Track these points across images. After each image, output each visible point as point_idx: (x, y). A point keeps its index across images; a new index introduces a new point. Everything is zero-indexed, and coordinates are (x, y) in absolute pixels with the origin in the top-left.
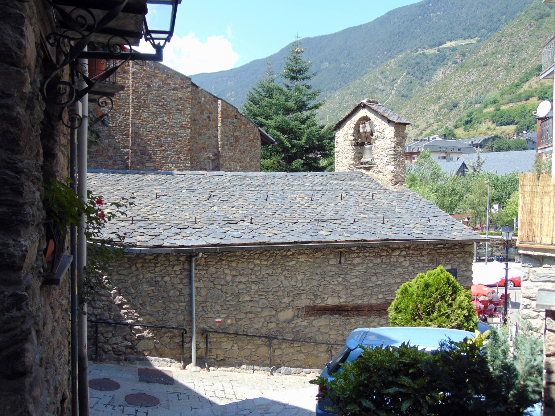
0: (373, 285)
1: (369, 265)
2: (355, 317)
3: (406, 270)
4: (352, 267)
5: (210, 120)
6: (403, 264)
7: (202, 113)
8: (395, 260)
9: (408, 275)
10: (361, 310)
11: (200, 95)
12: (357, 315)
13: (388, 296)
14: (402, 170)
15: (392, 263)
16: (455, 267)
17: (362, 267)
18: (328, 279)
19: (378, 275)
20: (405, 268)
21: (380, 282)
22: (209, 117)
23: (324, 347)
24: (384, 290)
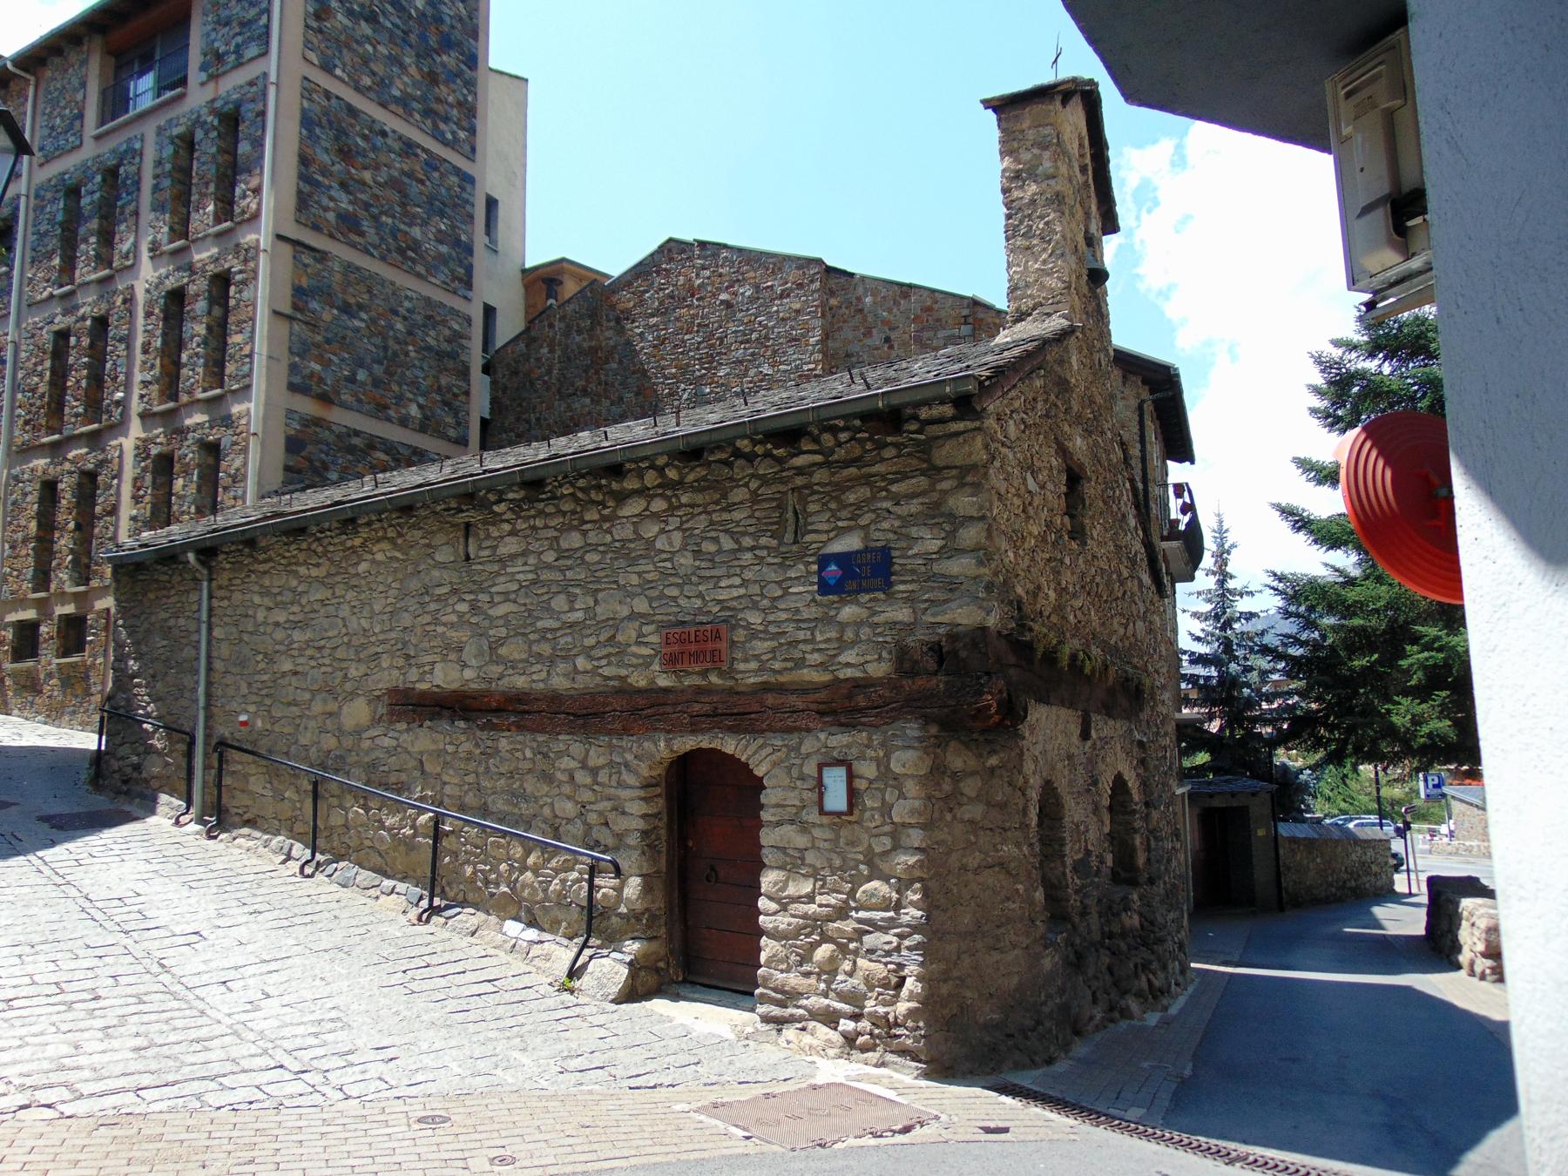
2: (513, 733)
3: (668, 565)
4: (496, 567)
5: (891, 347)
7: (868, 334)
8: (627, 532)
9: (677, 585)
10: (528, 712)
11: (860, 290)
12: (520, 728)
13: (604, 662)
14: (1044, 262)
15: (617, 544)
16: (880, 537)
17: (525, 564)
18: (433, 606)
19: (571, 589)
21: (579, 615)
22: (887, 340)
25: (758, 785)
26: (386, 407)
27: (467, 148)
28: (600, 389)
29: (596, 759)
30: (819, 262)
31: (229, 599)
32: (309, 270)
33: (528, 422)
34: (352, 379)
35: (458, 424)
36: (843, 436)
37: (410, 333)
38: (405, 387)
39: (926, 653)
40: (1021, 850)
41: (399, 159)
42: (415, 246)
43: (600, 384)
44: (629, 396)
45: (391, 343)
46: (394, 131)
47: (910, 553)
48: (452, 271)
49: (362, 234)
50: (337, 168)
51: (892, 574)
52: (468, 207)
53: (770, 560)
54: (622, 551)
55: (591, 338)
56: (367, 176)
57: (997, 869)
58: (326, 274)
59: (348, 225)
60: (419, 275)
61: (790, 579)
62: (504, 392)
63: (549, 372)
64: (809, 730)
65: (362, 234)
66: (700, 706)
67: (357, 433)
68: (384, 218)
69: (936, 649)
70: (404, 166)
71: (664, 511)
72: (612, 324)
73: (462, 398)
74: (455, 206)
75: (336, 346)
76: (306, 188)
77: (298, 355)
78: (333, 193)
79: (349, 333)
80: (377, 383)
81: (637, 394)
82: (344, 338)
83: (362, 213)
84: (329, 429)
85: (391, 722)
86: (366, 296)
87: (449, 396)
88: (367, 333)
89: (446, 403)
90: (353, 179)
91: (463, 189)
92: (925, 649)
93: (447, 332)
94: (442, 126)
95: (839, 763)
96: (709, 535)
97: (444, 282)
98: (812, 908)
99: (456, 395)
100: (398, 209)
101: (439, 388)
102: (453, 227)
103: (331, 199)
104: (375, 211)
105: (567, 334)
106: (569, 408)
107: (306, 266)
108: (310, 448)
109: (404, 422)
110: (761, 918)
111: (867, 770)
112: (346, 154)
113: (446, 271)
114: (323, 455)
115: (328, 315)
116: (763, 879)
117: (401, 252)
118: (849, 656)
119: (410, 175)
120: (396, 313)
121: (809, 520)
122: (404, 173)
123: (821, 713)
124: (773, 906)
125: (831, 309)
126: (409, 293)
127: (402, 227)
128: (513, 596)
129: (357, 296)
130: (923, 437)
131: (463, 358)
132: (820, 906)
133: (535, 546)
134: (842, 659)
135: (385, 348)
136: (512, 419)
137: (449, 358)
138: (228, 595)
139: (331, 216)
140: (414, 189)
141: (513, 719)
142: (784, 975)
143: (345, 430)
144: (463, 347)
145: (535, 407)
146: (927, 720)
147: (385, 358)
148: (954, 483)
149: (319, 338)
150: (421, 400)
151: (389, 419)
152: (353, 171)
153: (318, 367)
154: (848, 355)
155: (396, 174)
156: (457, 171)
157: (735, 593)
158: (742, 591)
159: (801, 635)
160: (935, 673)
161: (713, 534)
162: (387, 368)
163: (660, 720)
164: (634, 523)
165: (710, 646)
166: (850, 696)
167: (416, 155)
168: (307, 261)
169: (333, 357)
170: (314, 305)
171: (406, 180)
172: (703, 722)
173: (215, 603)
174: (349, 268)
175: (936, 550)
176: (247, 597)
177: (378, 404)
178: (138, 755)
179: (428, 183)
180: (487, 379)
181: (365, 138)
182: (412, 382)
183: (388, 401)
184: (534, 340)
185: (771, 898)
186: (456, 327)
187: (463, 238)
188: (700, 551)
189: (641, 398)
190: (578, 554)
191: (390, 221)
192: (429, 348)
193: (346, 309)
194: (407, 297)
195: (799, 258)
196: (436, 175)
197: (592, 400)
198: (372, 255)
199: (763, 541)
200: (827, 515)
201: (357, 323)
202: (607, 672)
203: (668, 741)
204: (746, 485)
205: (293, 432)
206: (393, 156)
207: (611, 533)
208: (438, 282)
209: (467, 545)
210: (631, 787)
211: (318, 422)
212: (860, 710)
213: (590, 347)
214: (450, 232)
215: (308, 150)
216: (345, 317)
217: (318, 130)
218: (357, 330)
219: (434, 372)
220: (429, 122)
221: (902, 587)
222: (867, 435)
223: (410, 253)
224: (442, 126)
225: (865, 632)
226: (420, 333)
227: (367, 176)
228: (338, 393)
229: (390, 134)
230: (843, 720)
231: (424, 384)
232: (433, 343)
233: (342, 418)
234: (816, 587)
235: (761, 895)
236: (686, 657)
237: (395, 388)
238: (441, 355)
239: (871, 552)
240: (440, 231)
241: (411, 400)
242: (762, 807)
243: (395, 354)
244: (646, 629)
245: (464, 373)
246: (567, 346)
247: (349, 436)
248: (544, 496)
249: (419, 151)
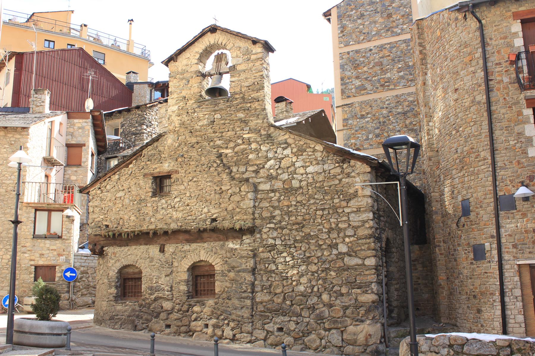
42: (389, 80)
49: (366, 89)
56: (365, 69)
93: (407, 103)
97: (403, 86)
101: (406, 125)
102: (405, 63)
117: (382, 86)
122: (381, 58)
126: (387, 98)
149: (353, 131)
152: (360, 71)
171: (381, 60)
192: (399, 113)
198: (371, 94)
224: (395, 30)
227: (365, 69)
243: (384, 122)
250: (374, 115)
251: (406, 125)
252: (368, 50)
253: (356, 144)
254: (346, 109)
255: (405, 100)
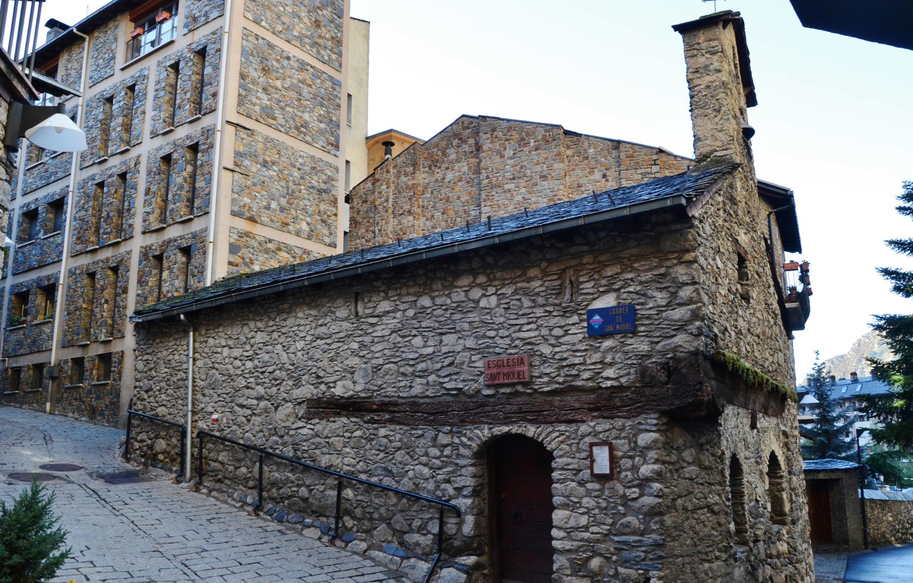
0: (416, 355)
1: (407, 314)
3: (488, 317)
5: (607, 180)
6: (483, 303)
8: (462, 296)
9: (495, 330)
11: (586, 145)
12: (391, 421)
13: (447, 379)
15: (455, 305)
17: (394, 318)
19: (424, 333)
20: (488, 313)
21: (430, 350)
23: (331, 481)
24: (439, 366)
25: (550, 456)
26: (287, 224)
27: (337, 64)
28: (419, 210)
29: (444, 439)
30: (559, 127)
31: (206, 342)
32: (244, 141)
33: (374, 232)
34: (268, 208)
35: (331, 234)
36: (602, 234)
37: (302, 178)
38: (299, 212)
39: (659, 371)
40: (721, 498)
41: (297, 73)
42: (305, 125)
43: (419, 207)
44: (438, 214)
45: (291, 184)
46: (294, 57)
47: (648, 307)
48: (327, 139)
49: (274, 119)
50: (261, 80)
51: (636, 320)
52: (337, 100)
53: (555, 314)
54: (459, 307)
55: (413, 179)
56: (278, 84)
57: (706, 510)
58: (253, 143)
59: (267, 114)
60: (307, 143)
61: (569, 324)
62: (358, 214)
63: (387, 201)
64: (583, 422)
65: (274, 119)
66: (510, 407)
67: (270, 241)
68: (288, 109)
69: (665, 366)
70: (300, 76)
71: (484, 283)
72: (427, 169)
73: (333, 218)
74: (330, 99)
75: (259, 187)
76: (243, 93)
77: (237, 193)
78: (259, 94)
79: (266, 179)
80: (282, 209)
81: (443, 213)
82: (263, 182)
83: (275, 106)
84: (254, 238)
85: (309, 419)
86: (277, 156)
87: (325, 217)
88: (277, 178)
89: (323, 221)
90: (270, 86)
91: (334, 89)
92: (659, 368)
93: (324, 177)
94: (322, 52)
95: (603, 443)
96: (514, 298)
98: (586, 535)
99: (329, 216)
100: (296, 103)
101: (319, 212)
102: (328, 112)
103: (257, 98)
104: (283, 104)
105: (398, 177)
106: (400, 223)
107: (242, 139)
108: (243, 251)
109: (298, 234)
110: (554, 542)
111: (622, 445)
112: (266, 71)
113: (324, 140)
114: (251, 255)
115: (255, 168)
116: (554, 516)
117: (297, 128)
118: (610, 372)
119: (303, 82)
120: (294, 166)
121: (581, 287)
123: (591, 410)
124: (562, 534)
125: (567, 157)
126: (302, 154)
127: (299, 114)
128: (386, 338)
129: (271, 156)
130: (653, 234)
131: (333, 192)
132: (592, 533)
133: (402, 307)
134: (604, 374)
135: (288, 188)
136: (363, 230)
137: (324, 192)
138: (206, 339)
139: (257, 108)
140: (305, 90)
141: (387, 416)
142: (569, 578)
143: (263, 239)
144: (333, 186)
145: (378, 223)
146: (663, 413)
147: (287, 194)
148: (675, 261)
150: (308, 220)
151: (289, 232)
152: (271, 81)
153: (248, 201)
154: (579, 186)
155: (295, 81)
156: (331, 78)
157: (532, 334)
158: (536, 333)
159: (577, 361)
160: (667, 383)
161: (517, 297)
162: (289, 200)
163: (483, 417)
164: (464, 291)
165: (517, 369)
166: (610, 398)
167: (307, 70)
168: (243, 136)
169: (257, 194)
170: (246, 162)
171: (301, 85)
172: (513, 417)
173: (197, 345)
174: (267, 140)
175: (664, 304)
176: (217, 341)
177: (283, 223)
178: (151, 439)
179: (314, 86)
180: (348, 206)
181: (277, 61)
182: (303, 209)
183: (289, 221)
184: (378, 180)
185: (560, 528)
186: (330, 174)
187: (334, 119)
188: (509, 308)
189: (445, 216)
190: (429, 311)
191: (291, 110)
193: (265, 164)
194: (300, 156)
195: (546, 125)
196: (319, 81)
197: (414, 217)
199: (551, 301)
200: (592, 283)
201: (271, 173)
202: (448, 386)
203: (490, 429)
204: (538, 266)
205: (234, 241)
206: (293, 71)
207: (450, 298)
208: (319, 147)
209: (356, 307)
210: (467, 457)
211: (247, 234)
212: (617, 408)
213: (413, 184)
214: (326, 116)
215: (246, 70)
216: (264, 169)
217: (251, 58)
218: (271, 177)
219: (316, 201)
220: (315, 50)
221: (642, 328)
222: (617, 233)
223: (302, 129)
224: (322, 52)
225: (619, 356)
226: (308, 178)
227: (278, 84)
228: (260, 216)
229: (292, 59)
230: (605, 414)
231: (310, 210)
232: (316, 184)
233: (261, 231)
234: (586, 330)
235: (553, 527)
236: (501, 376)
237: (293, 212)
238: (320, 191)
239: (622, 307)
240: (320, 115)
241: (302, 220)
242: (552, 470)
243: (293, 191)
244: (474, 358)
245: (335, 202)
246: (398, 184)
247: (266, 243)
248: (406, 276)
249: (309, 67)
250: (281, 172)
251: (319, 212)
252: (285, 54)
253: (250, 207)
254: (243, 134)
255: (322, 171)
